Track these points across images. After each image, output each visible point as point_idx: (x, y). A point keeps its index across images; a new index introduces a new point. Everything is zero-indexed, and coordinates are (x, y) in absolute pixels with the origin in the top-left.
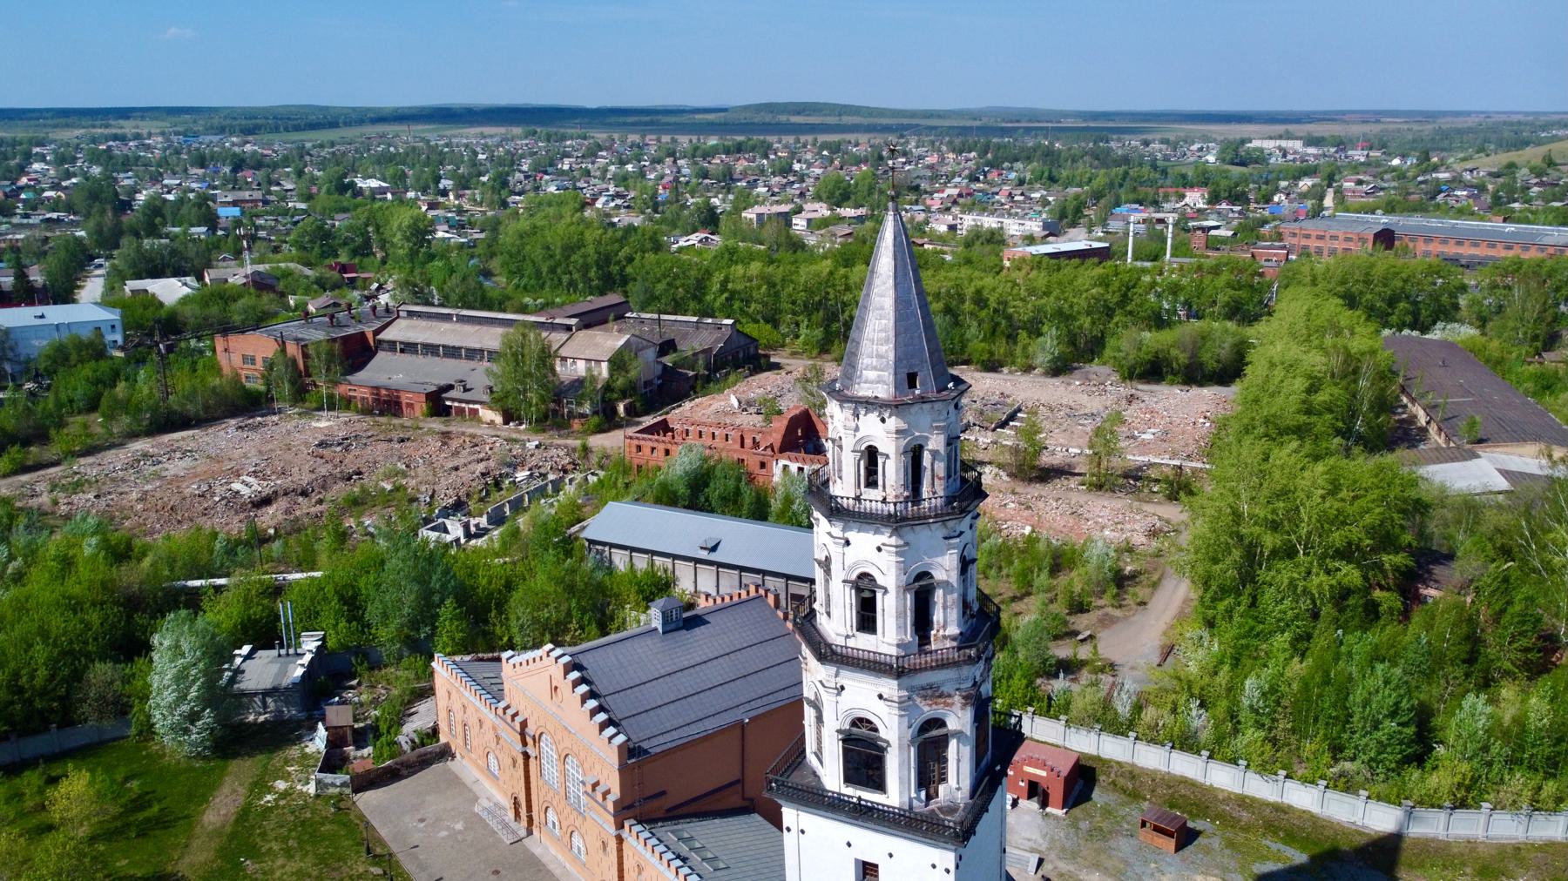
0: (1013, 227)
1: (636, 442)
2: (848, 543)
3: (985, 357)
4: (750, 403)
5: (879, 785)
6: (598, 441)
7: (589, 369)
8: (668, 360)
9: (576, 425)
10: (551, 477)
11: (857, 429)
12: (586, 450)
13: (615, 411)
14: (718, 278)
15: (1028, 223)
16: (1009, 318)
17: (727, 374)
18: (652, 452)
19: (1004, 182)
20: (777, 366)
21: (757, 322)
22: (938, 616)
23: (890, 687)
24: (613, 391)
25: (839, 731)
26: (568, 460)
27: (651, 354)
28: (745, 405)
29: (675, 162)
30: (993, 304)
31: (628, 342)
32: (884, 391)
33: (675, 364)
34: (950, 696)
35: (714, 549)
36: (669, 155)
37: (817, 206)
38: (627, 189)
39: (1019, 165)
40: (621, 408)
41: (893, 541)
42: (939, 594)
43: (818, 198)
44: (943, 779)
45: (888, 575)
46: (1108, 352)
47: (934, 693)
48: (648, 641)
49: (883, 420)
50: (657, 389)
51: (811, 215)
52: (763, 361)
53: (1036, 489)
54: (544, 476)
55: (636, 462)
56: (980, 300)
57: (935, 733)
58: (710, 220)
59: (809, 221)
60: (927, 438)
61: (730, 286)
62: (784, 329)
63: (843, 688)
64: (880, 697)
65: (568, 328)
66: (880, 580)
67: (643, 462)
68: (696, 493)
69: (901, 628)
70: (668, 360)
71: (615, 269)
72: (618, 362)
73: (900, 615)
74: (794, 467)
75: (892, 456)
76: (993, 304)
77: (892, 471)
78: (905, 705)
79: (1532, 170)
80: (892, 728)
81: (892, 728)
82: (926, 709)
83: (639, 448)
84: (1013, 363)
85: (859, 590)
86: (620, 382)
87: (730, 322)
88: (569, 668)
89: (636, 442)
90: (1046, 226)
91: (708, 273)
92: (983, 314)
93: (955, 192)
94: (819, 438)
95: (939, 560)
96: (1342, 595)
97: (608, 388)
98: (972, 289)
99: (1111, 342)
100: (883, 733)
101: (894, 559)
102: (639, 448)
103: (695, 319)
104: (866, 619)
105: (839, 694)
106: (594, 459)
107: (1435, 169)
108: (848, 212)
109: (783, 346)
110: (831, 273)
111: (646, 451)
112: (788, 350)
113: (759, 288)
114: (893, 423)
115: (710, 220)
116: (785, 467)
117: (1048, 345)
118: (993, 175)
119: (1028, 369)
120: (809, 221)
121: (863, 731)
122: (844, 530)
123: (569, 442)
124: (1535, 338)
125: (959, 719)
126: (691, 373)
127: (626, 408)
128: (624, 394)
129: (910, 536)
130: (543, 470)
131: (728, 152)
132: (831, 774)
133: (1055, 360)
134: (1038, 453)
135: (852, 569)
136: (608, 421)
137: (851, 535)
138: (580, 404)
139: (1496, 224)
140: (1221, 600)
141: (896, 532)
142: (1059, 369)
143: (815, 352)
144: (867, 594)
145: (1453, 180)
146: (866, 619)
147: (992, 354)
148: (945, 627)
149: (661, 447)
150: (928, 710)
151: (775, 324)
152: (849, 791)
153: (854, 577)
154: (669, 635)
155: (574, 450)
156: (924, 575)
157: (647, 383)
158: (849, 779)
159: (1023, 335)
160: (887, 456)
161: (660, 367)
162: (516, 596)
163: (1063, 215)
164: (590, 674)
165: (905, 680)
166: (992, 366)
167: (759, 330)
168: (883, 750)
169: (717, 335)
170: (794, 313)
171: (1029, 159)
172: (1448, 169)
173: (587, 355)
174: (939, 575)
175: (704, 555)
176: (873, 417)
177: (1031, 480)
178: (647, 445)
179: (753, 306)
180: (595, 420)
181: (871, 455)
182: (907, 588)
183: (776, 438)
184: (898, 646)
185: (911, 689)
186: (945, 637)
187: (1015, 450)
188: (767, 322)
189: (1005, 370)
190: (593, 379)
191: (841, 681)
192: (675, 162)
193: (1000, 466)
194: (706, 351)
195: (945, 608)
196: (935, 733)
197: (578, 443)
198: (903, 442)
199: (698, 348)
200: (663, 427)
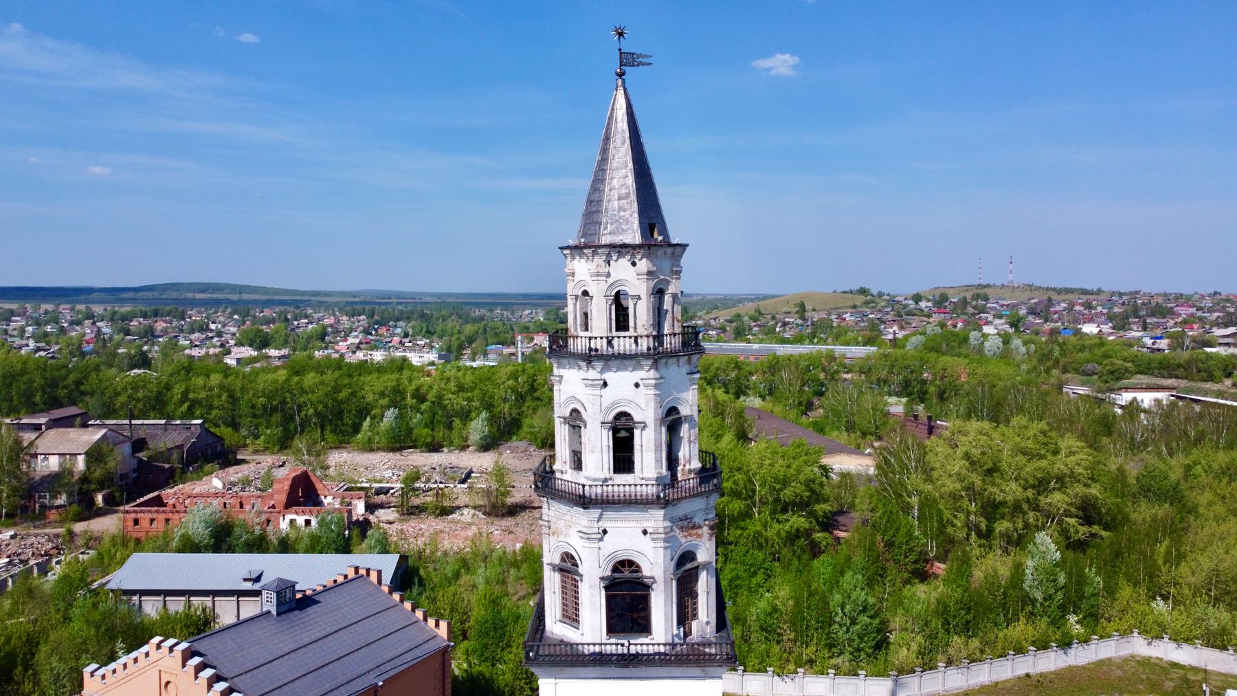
0: (415, 359)
1: (133, 516)
2: (605, 384)
3: (429, 440)
4: (233, 484)
5: (643, 627)
6: (79, 527)
7: (61, 465)
8: (143, 455)
9: (53, 515)
10: (32, 562)
11: (608, 275)
12: (71, 534)
13: (92, 501)
14: (178, 390)
15: (426, 356)
16: (444, 408)
17: (201, 467)
18: (150, 522)
19: (393, 335)
20: (243, 462)
21: (217, 426)
22: (683, 452)
23: (656, 519)
24: (89, 482)
25: (602, 579)
26: (50, 545)
27: (127, 448)
28: (229, 486)
29: (94, 323)
30: (431, 396)
31: (104, 436)
32: (633, 236)
33: (150, 457)
34: (700, 527)
35: (257, 579)
36: (88, 318)
37: (243, 349)
38: (48, 344)
39: (401, 323)
40: (99, 498)
41: (652, 373)
42: (685, 428)
43: (239, 344)
44: (695, 616)
45: (645, 410)
46: (525, 428)
47: (688, 524)
48: (264, 623)
49: (634, 264)
50: (138, 479)
51: (239, 356)
52: (231, 456)
53: (508, 522)
54: (25, 562)
55: (135, 535)
56: (421, 398)
57: (689, 566)
58: (143, 361)
59: (238, 360)
60: (668, 282)
61: (191, 396)
62: (244, 432)
63: (605, 532)
64: (645, 532)
65: (37, 427)
66: (637, 417)
67: (140, 535)
68: (222, 538)
69: (658, 461)
70: (143, 455)
71: (62, 392)
72: (95, 455)
73: (658, 449)
74: (301, 520)
75: (644, 297)
76: (431, 396)
77: (641, 315)
78: (669, 539)
79: (751, 318)
81: (655, 563)
82: (683, 540)
83: (136, 522)
84: (451, 444)
85: (615, 430)
86: (98, 473)
87: (199, 421)
88: (188, 655)
89: (133, 516)
90: (440, 357)
91: (168, 387)
92: (424, 407)
93: (357, 341)
94: (318, 495)
95: (684, 395)
96: (793, 537)
97: (85, 479)
98: (412, 388)
99: (527, 421)
100: (646, 571)
101: (652, 392)
102: (136, 522)
103: (163, 422)
104: (623, 459)
105: (601, 540)
106: (80, 541)
107: (692, 318)
108: (273, 352)
109: (245, 446)
110: (286, 380)
111: (145, 523)
112: (250, 449)
113: (219, 396)
114: (643, 265)
115: (143, 361)
116: (292, 521)
117: (478, 427)
118: (383, 330)
119: (464, 448)
120: (238, 360)
121: (627, 574)
122: (601, 372)
123: (47, 531)
124: (800, 404)
125: (705, 552)
126: (167, 466)
127: (104, 499)
128: (102, 485)
129: (663, 370)
130: (22, 557)
131: (145, 316)
132: (593, 629)
133: (484, 438)
134: (506, 494)
135: (609, 409)
136: (88, 511)
137: (608, 376)
138: (54, 497)
139: (742, 345)
141: (655, 366)
142: (487, 445)
143: (276, 449)
144: (623, 434)
145: (705, 325)
146: (623, 459)
147: (433, 437)
148: (690, 462)
149: (162, 517)
150: (685, 541)
151: (236, 427)
152: (613, 641)
153: (611, 418)
154: (284, 616)
155: (57, 536)
156: (673, 410)
157: (123, 477)
158: (612, 629)
159: (457, 422)
160: (639, 298)
161: (135, 461)
162: (44, 649)
163: (449, 350)
164: (211, 659)
165: (670, 508)
166: (434, 448)
167: (225, 432)
168: (647, 588)
169: (186, 434)
170: (254, 416)
171: (409, 319)
172: (700, 318)
173: (61, 449)
174: (684, 411)
175: (248, 586)
176: (624, 262)
177: (503, 516)
178: (145, 518)
179: (214, 412)
180: (75, 508)
182: (662, 421)
183: (282, 498)
184: (657, 479)
185: (672, 520)
186: (690, 471)
187: (488, 493)
188: (228, 425)
189: (445, 450)
190: (71, 473)
191: (604, 524)
192: (94, 323)
193: (475, 508)
194: (180, 447)
195: (690, 442)
196: (689, 566)
197: (61, 530)
198: (652, 284)
199: (170, 445)
200: (158, 502)
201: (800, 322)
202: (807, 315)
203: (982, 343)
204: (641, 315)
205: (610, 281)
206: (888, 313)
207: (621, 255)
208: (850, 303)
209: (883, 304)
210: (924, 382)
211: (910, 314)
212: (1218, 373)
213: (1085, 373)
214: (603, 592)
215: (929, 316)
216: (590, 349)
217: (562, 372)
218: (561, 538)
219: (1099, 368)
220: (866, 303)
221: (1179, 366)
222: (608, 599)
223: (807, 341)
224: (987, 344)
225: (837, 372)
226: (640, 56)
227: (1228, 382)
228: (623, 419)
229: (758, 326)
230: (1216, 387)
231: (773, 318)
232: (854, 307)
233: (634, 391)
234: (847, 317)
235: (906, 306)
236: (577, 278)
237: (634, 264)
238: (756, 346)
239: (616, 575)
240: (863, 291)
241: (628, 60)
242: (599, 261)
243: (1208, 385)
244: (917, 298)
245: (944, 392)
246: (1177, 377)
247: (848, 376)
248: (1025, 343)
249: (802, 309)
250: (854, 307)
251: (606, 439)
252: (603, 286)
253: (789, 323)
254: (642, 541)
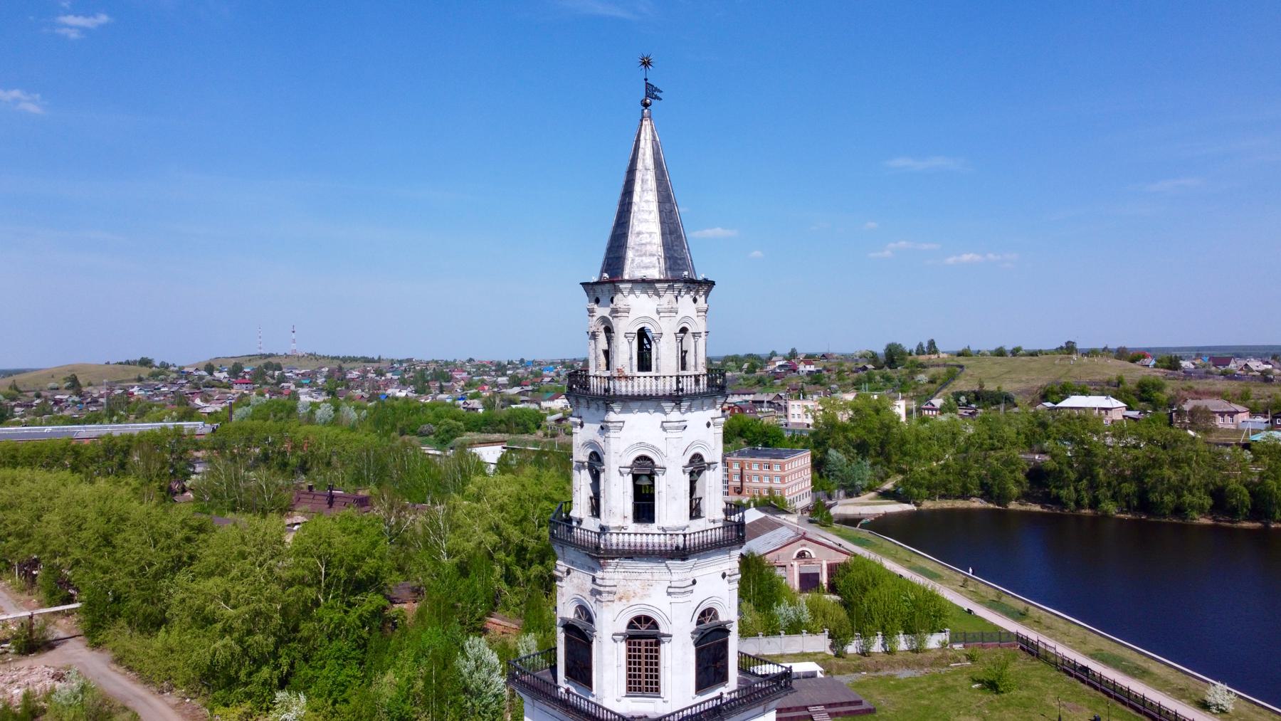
49: (695, 300)
80: (729, 612)
100: (722, 618)
140: (257, 671)
153: (686, 462)
158: (701, 686)
201: (76, 399)
202: (84, 390)
203: (312, 412)
204: (665, 355)
206: (182, 385)
207: (689, 290)
208: (133, 376)
209: (175, 375)
210: (284, 454)
211: (208, 385)
212: (532, 426)
213: (422, 434)
214: (693, 648)
215: (230, 387)
216: (678, 390)
217: (622, 417)
218: (633, 601)
219: (435, 429)
220: (154, 376)
221: (501, 422)
222: (699, 653)
223: (106, 420)
224: (319, 412)
225: (185, 451)
226: (657, 90)
227: (540, 433)
228: (697, 462)
229: (20, 406)
230: (532, 438)
231: (38, 396)
232: (140, 379)
233: (703, 429)
234: (135, 390)
235: (201, 378)
236: (632, 316)
237: (695, 300)
238: (49, 429)
239: (702, 626)
240: (145, 362)
241: (651, 92)
242: (669, 296)
243: (526, 437)
244: (210, 369)
245: (306, 463)
246: (499, 432)
247: (199, 454)
248: (357, 408)
249: (74, 384)
250: (140, 379)
253: (61, 401)
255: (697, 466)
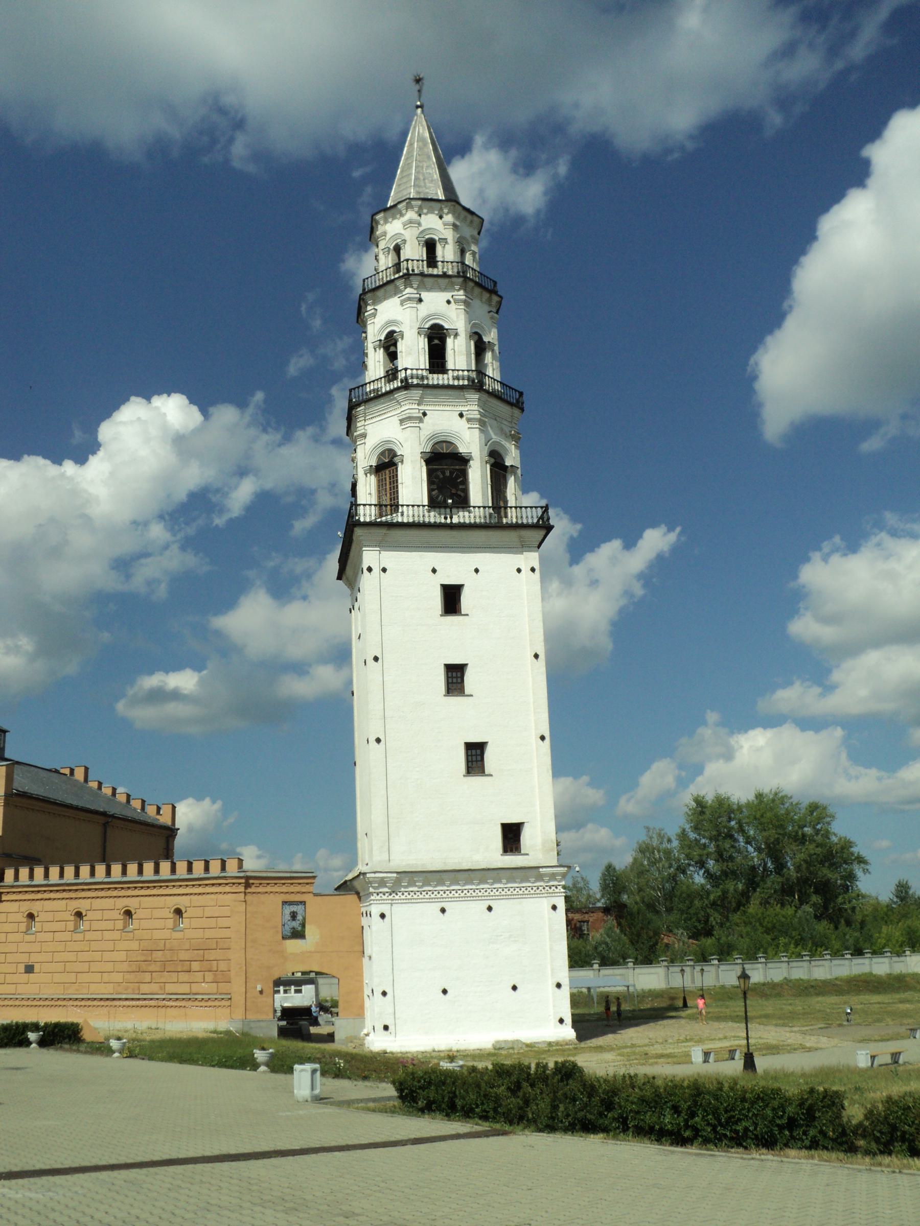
2: (420, 300)
5: (463, 502)
49: (441, 217)
63: (425, 414)
85: (430, 339)
100: (462, 449)
137: (425, 295)
181: (431, 246)
205: (421, 229)
207: (431, 211)
214: (424, 469)
222: (430, 473)
251: (423, 343)
252: (416, 232)
254: (459, 425)
255: (437, 338)
